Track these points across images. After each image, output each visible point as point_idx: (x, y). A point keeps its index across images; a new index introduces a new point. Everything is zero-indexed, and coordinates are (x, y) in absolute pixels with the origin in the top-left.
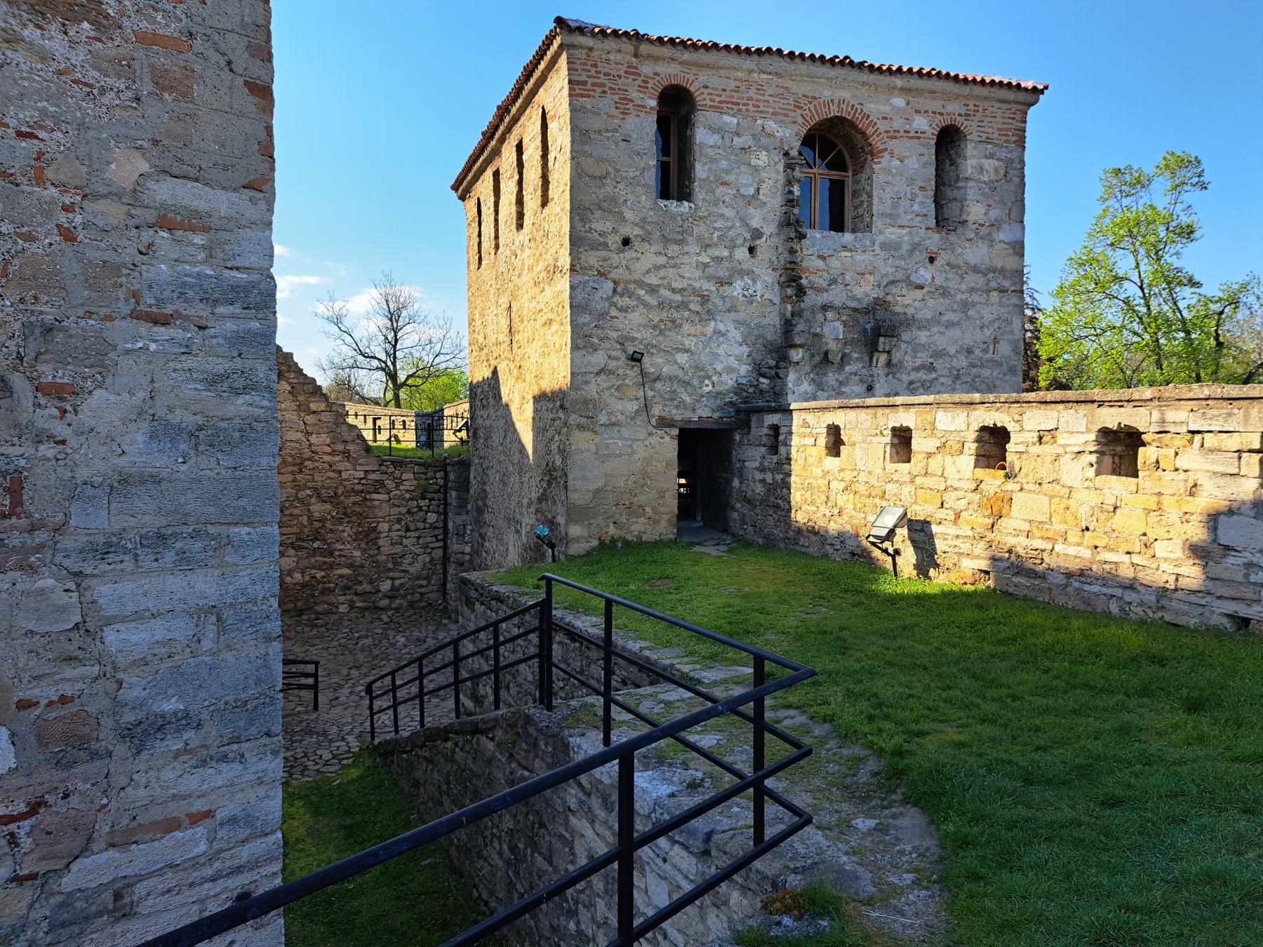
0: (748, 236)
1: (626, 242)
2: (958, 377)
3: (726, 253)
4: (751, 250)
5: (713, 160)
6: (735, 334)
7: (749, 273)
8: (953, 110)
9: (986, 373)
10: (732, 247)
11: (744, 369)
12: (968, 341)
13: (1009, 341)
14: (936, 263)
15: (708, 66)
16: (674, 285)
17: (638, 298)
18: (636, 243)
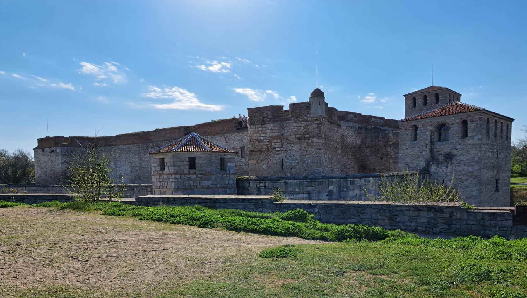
0: (425, 145)
1: (407, 148)
2: (465, 164)
3: (422, 148)
4: (426, 147)
5: (420, 135)
6: (423, 160)
7: (426, 150)
8: (464, 117)
9: (472, 163)
10: (423, 147)
11: (424, 165)
12: (468, 157)
13: (478, 157)
14: (461, 145)
15: (418, 122)
16: (414, 154)
17: (408, 156)
18: (408, 148)
